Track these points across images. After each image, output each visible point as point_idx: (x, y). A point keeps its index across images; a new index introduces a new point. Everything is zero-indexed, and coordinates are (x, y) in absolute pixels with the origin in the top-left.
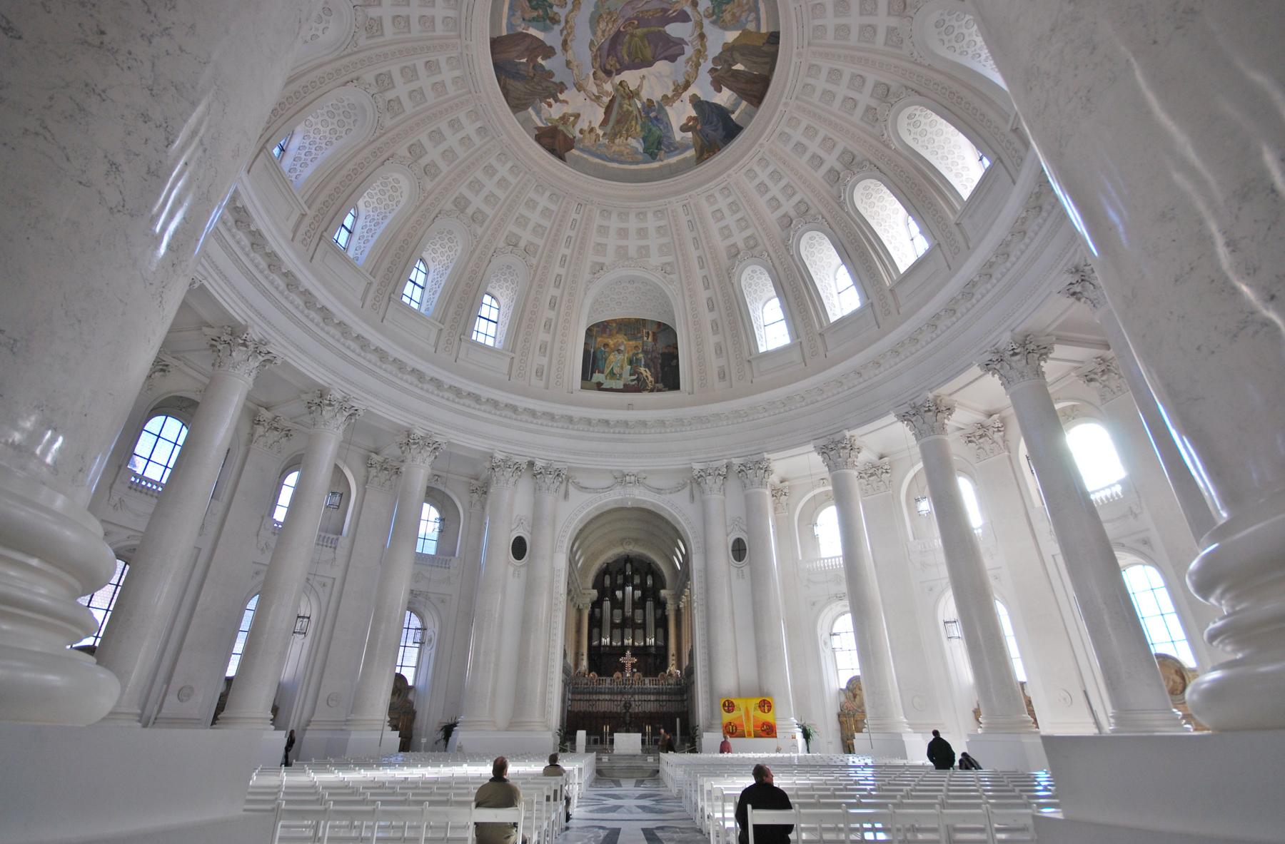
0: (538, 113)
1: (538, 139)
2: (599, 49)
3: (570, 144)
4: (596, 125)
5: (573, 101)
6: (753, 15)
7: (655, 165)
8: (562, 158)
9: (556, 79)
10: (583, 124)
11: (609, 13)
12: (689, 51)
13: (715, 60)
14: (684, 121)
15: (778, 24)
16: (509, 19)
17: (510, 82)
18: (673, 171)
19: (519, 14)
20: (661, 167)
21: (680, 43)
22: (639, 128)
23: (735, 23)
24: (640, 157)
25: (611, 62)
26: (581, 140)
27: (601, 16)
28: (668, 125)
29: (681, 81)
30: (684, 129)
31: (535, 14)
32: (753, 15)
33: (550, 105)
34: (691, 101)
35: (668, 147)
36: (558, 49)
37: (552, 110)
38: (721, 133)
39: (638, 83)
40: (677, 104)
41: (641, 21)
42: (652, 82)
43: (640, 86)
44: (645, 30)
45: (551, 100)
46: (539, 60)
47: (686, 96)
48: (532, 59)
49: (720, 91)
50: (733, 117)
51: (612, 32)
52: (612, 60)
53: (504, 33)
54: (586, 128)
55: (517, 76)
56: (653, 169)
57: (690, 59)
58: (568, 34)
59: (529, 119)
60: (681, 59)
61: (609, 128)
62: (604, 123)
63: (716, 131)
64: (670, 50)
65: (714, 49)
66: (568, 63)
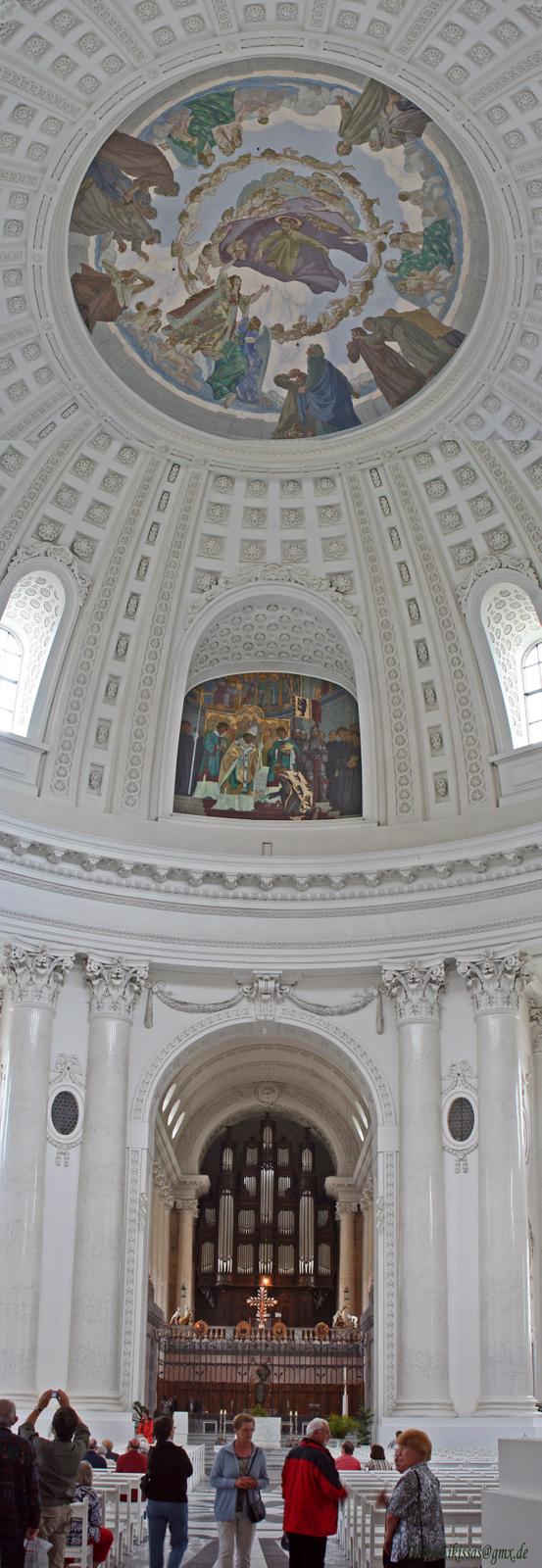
0: (101, 248)
1: (75, 280)
2: (233, 223)
3: (113, 312)
4: (166, 308)
5: (157, 261)
6: (441, 300)
7: (214, 407)
8: (89, 324)
9: (154, 224)
10: (148, 298)
11: (274, 194)
12: (342, 293)
13: (368, 321)
14: (287, 372)
15: (469, 325)
16: (154, 123)
17: (95, 190)
18: (234, 430)
19: (169, 127)
20: (219, 415)
21: (338, 277)
22: (220, 346)
23: (416, 295)
24: (199, 386)
25: (238, 247)
26: (132, 317)
27: (262, 191)
28: (261, 365)
29: (312, 321)
30: (280, 381)
32: (441, 300)
33: (123, 249)
34: (310, 352)
35: (244, 393)
36: (185, 191)
37: (120, 256)
38: (329, 412)
39: (255, 290)
40: (290, 345)
41: (307, 225)
42: (276, 301)
43: (255, 296)
44: (306, 238)
45: (129, 244)
46: (151, 190)
47: (308, 341)
48: (143, 184)
49: (354, 360)
50: (355, 402)
51: (263, 215)
52: (240, 246)
53: (135, 134)
54: (150, 303)
55: (109, 189)
56: (207, 412)
57: (338, 302)
58: (209, 185)
59: (83, 249)
60: (327, 295)
61: (178, 324)
62: (178, 313)
63: (323, 405)
64: (323, 278)
65: (374, 308)
66: (184, 215)
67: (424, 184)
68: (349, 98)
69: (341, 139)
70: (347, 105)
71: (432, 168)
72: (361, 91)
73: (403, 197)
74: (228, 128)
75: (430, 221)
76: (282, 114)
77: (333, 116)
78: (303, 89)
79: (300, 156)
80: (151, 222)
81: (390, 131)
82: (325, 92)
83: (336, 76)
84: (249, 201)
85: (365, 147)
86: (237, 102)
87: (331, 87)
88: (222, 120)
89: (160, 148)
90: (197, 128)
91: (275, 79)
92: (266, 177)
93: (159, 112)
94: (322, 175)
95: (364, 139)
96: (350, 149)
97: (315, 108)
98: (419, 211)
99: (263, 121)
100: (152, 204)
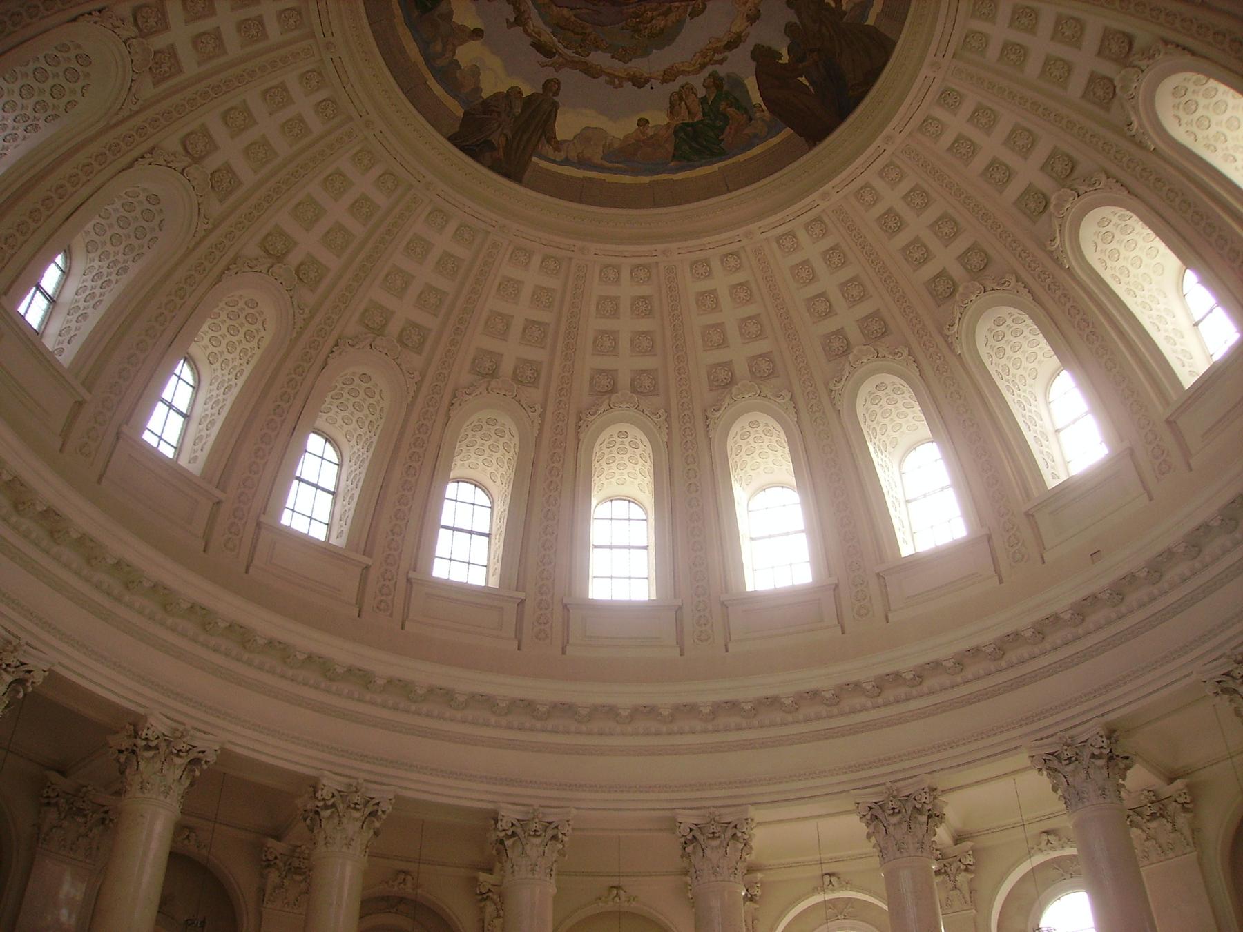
16: (765, 139)
31: (731, 111)
46: (785, 59)
53: (788, 131)
58: (716, 51)
66: (753, 18)
67: (454, 54)
68: (548, 150)
69: (556, 99)
70: (549, 142)
71: (448, 75)
72: (534, 159)
73: (477, 33)
75: (442, 8)
76: (620, 129)
77: (567, 125)
78: (597, 159)
79: (603, 79)
80: (795, 20)
81: (499, 113)
82: (573, 155)
84: (669, 24)
85: (527, 91)
86: (670, 147)
87: (566, 162)
90: (719, 123)
91: (626, 172)
92: (646, 53)
94: (577, 53)
95: (530, 97)
96: (545, 87)
97: (586, 136)
98: (457, 19)
99: (643, 123)
100: (788, 41)
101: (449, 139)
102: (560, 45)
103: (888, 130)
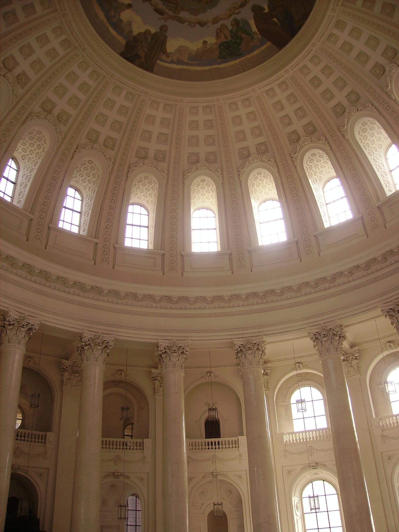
31: (244, 35)
46: (267, 10)
53: (269, 43)
67: (120, 16)
68: (164, 57)
69: (166, 34)
70: (164, 54)
72: (158, 62)
74: (223, 39)
76: (195, 46)
77: (172, 45)
78: (186, 60)
79: (186, 24)
83: (170, 68)
85: (153, 31)
87: (172, 62)
88: (226, 44)
89: (258, 33)
91: (198, 65)
93: (255, 53)
95: (155, 34)
97: (180, 50)
99: (205, 43)
101: (120, 55)
102: (166, 10)
103: (313, 41)
